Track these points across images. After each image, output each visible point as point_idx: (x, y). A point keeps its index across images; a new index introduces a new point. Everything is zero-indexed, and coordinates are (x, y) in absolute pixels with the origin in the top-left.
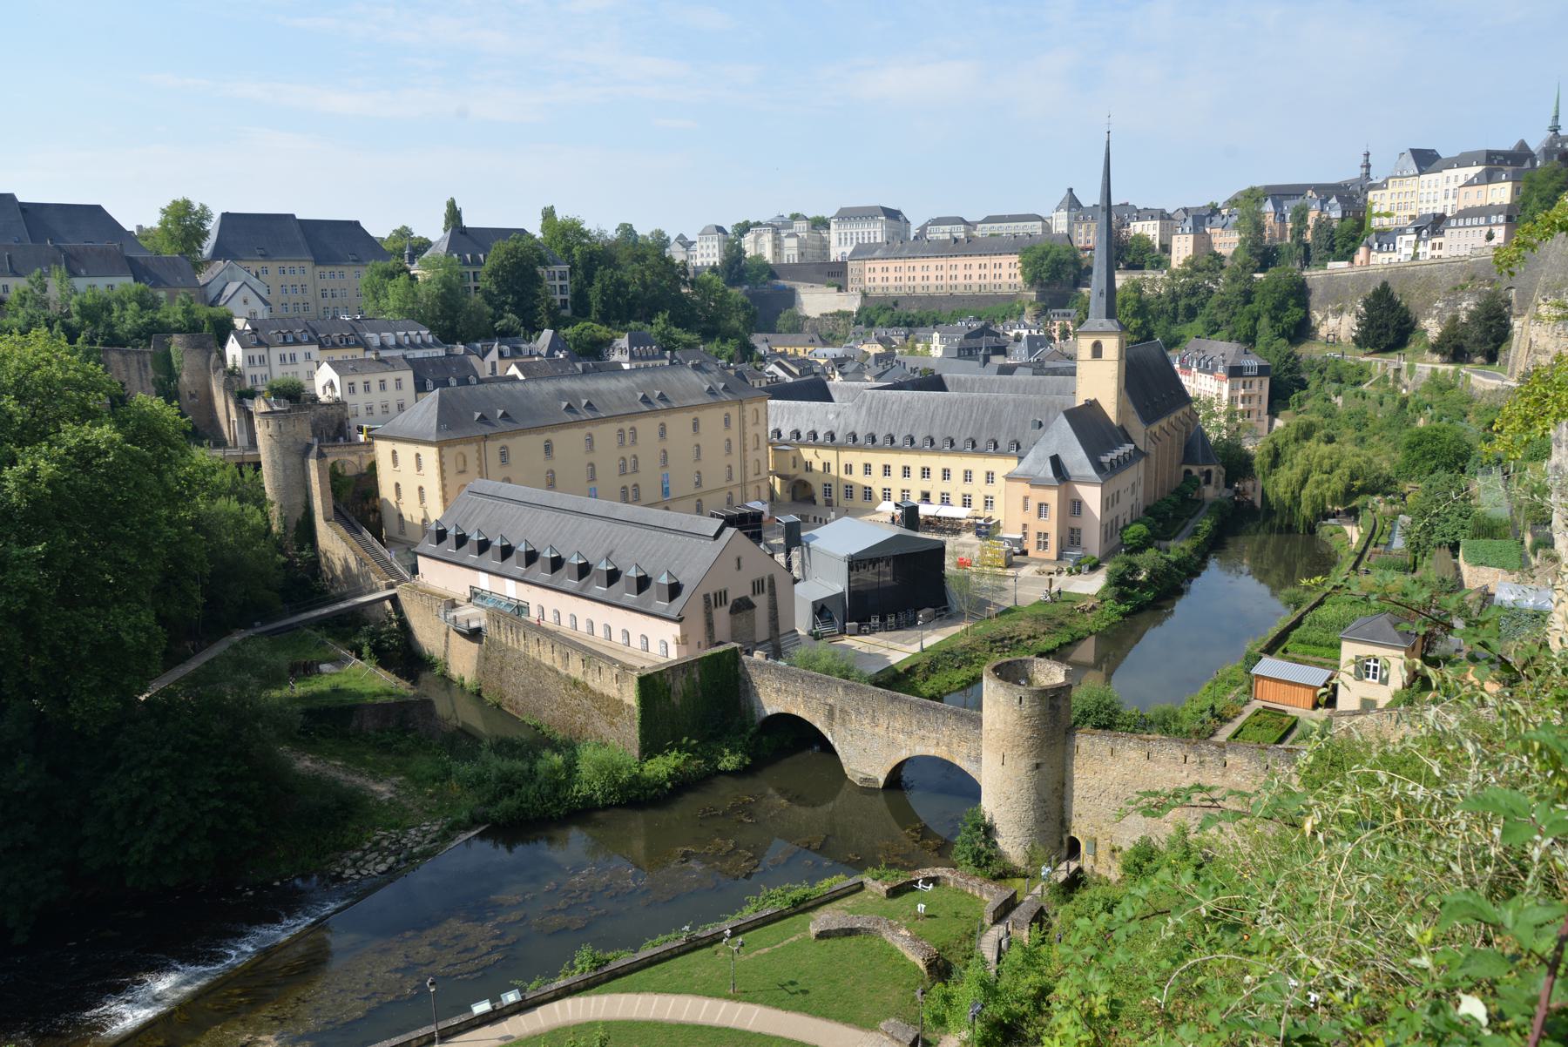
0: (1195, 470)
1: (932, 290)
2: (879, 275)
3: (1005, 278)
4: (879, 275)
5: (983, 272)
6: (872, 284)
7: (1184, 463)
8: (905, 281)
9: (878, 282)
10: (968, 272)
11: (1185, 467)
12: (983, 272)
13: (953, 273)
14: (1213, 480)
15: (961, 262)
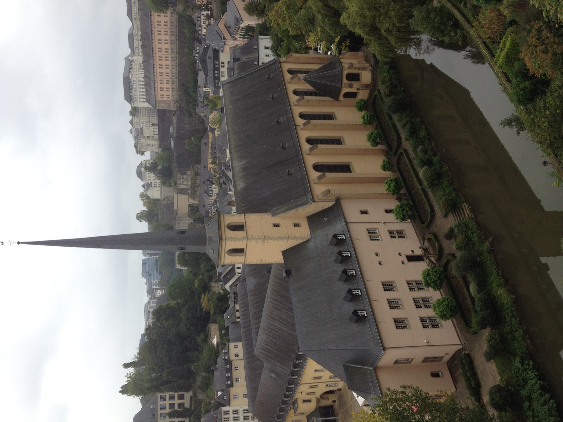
0: (345, 90)
1: (174, 63)
2: (165, 93)
3: (168, 37)
4: (165, 93)
5: (163, 33)
6: (171, 97)
7: (336, 98)
8: (169, 78)
9: (169, 93)
10: (163, 42)
11: (341, 98)
12: (163, 33)
13: (164, 50)
14: (356, 71)
15: (156, 46)
